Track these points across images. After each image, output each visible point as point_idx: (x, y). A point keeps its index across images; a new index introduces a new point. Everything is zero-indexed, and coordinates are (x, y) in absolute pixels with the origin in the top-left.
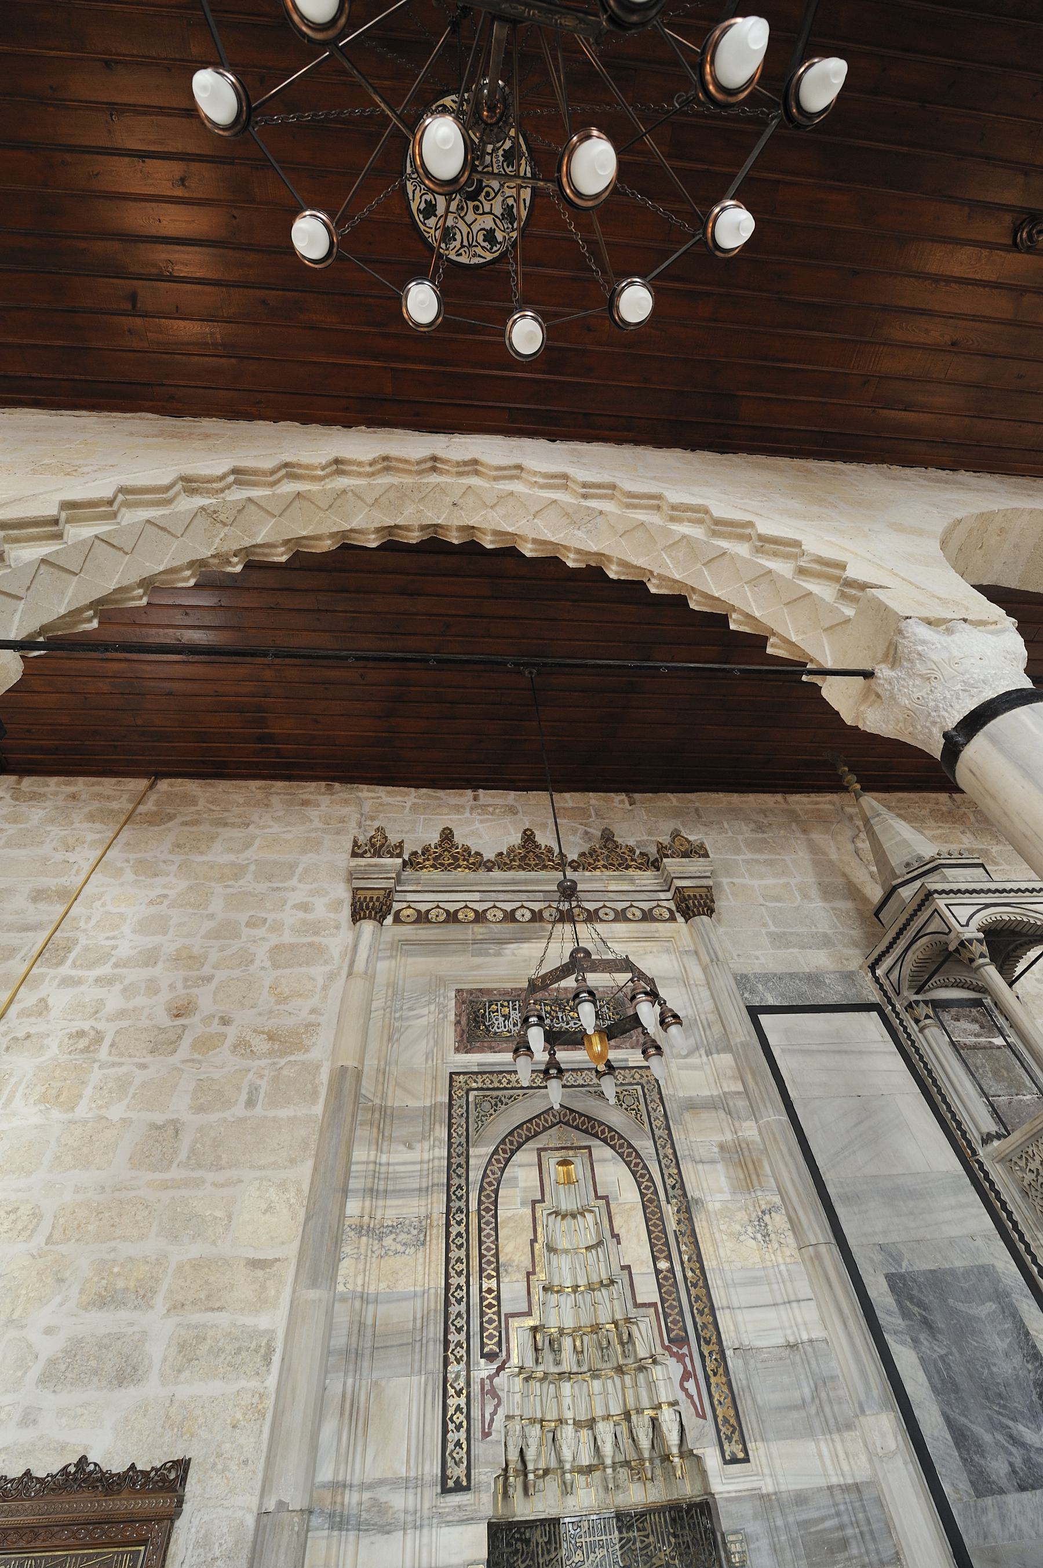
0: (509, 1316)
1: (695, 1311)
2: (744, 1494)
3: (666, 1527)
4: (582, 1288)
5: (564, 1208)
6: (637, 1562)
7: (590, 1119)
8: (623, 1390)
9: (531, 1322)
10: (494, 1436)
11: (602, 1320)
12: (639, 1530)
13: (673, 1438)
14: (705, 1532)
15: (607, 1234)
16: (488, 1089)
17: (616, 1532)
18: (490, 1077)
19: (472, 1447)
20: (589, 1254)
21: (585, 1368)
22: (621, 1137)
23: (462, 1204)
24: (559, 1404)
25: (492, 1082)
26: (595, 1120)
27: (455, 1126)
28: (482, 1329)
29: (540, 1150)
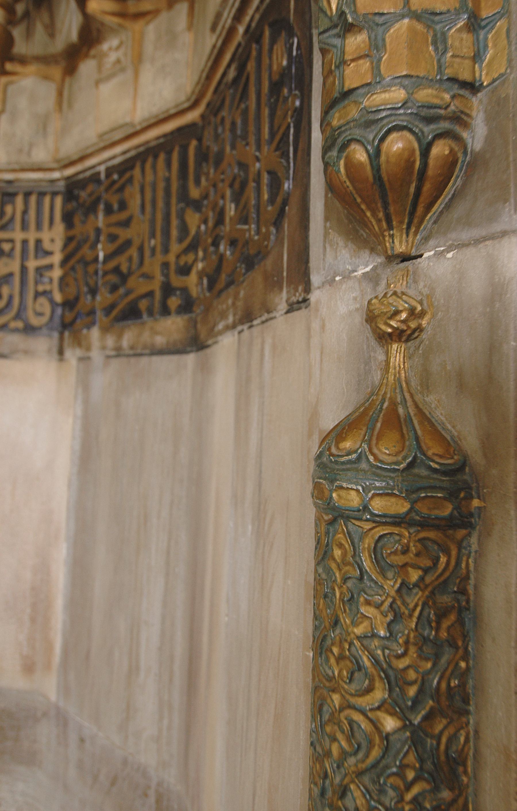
12: (109, 210)
17: (59, 228)
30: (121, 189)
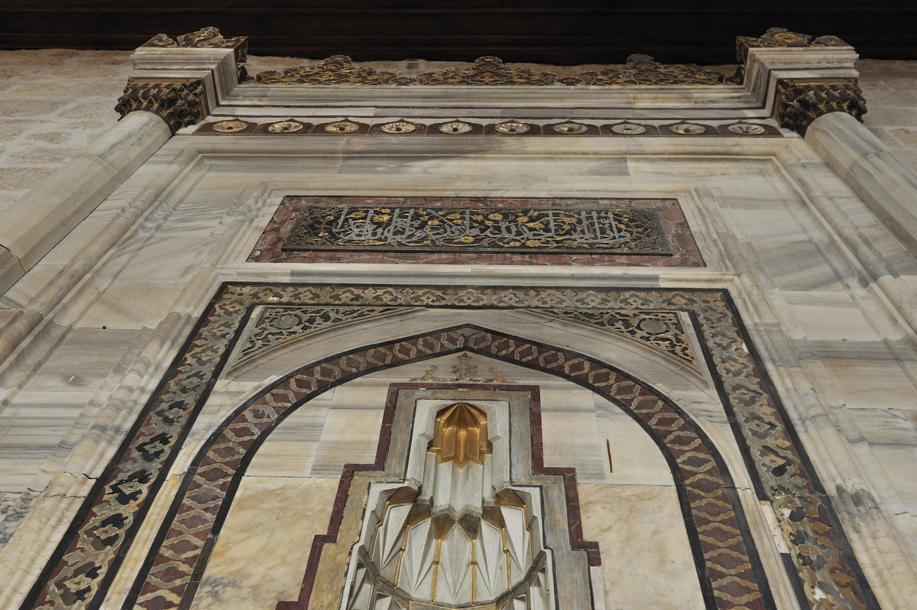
15: (561, 539)
29: (395, 390)
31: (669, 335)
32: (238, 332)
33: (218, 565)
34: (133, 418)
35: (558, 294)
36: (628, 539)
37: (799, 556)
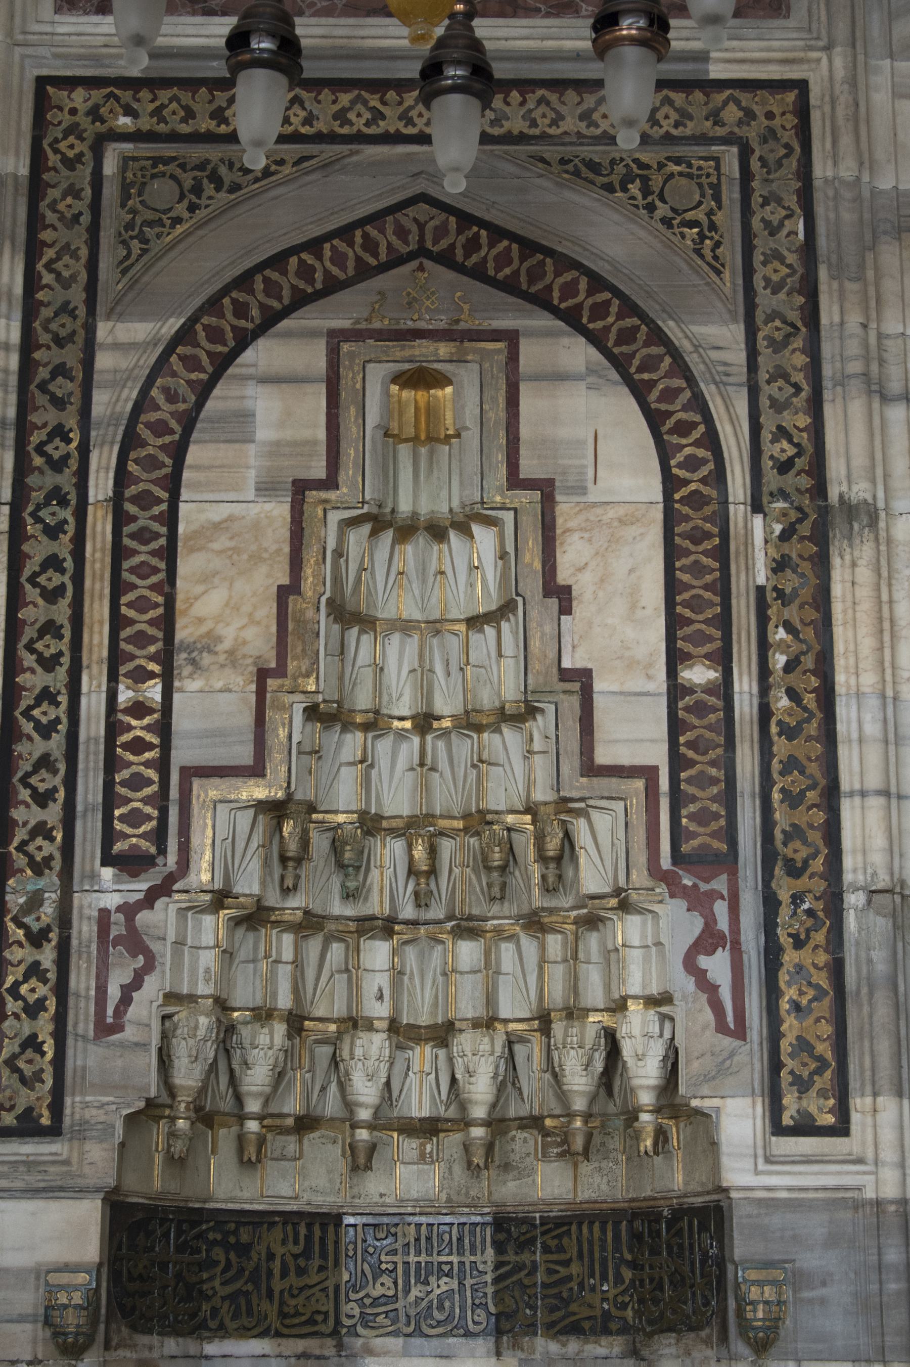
0: (190, 773)
1: (776, 796)
2: (811, 1195)
3: (617, 1249)
4: (446, 723)
5: (405, 506)
6: (534, 1308)
7: (529, 247)
8: (541, 968)
9: (259, 791)
10: (130, 1033)
11: (496, 800)
12: (546, 1250)
13: (644, 1072)
14: (703, 1262)
15: (533, 586)
16: (173, 137)
17: (490, 1252)
18: (186, 97)
19: (70, 1052)
20: (475, 637)
21: (437, 912)
22: (630, 308)
23: (66, 480)
24: (354, 989)
25: (190, 114)
26: (549, 252)
27: (50, 253)
28: (110, 799)
29: (336, 339)
30: (559, 1237)
31: (699, 215)
32: (96, 206)
33: (186, 627)
34: (13, 398)
35: (553, 97)
36: (602, 581)
37: (775, 588)
